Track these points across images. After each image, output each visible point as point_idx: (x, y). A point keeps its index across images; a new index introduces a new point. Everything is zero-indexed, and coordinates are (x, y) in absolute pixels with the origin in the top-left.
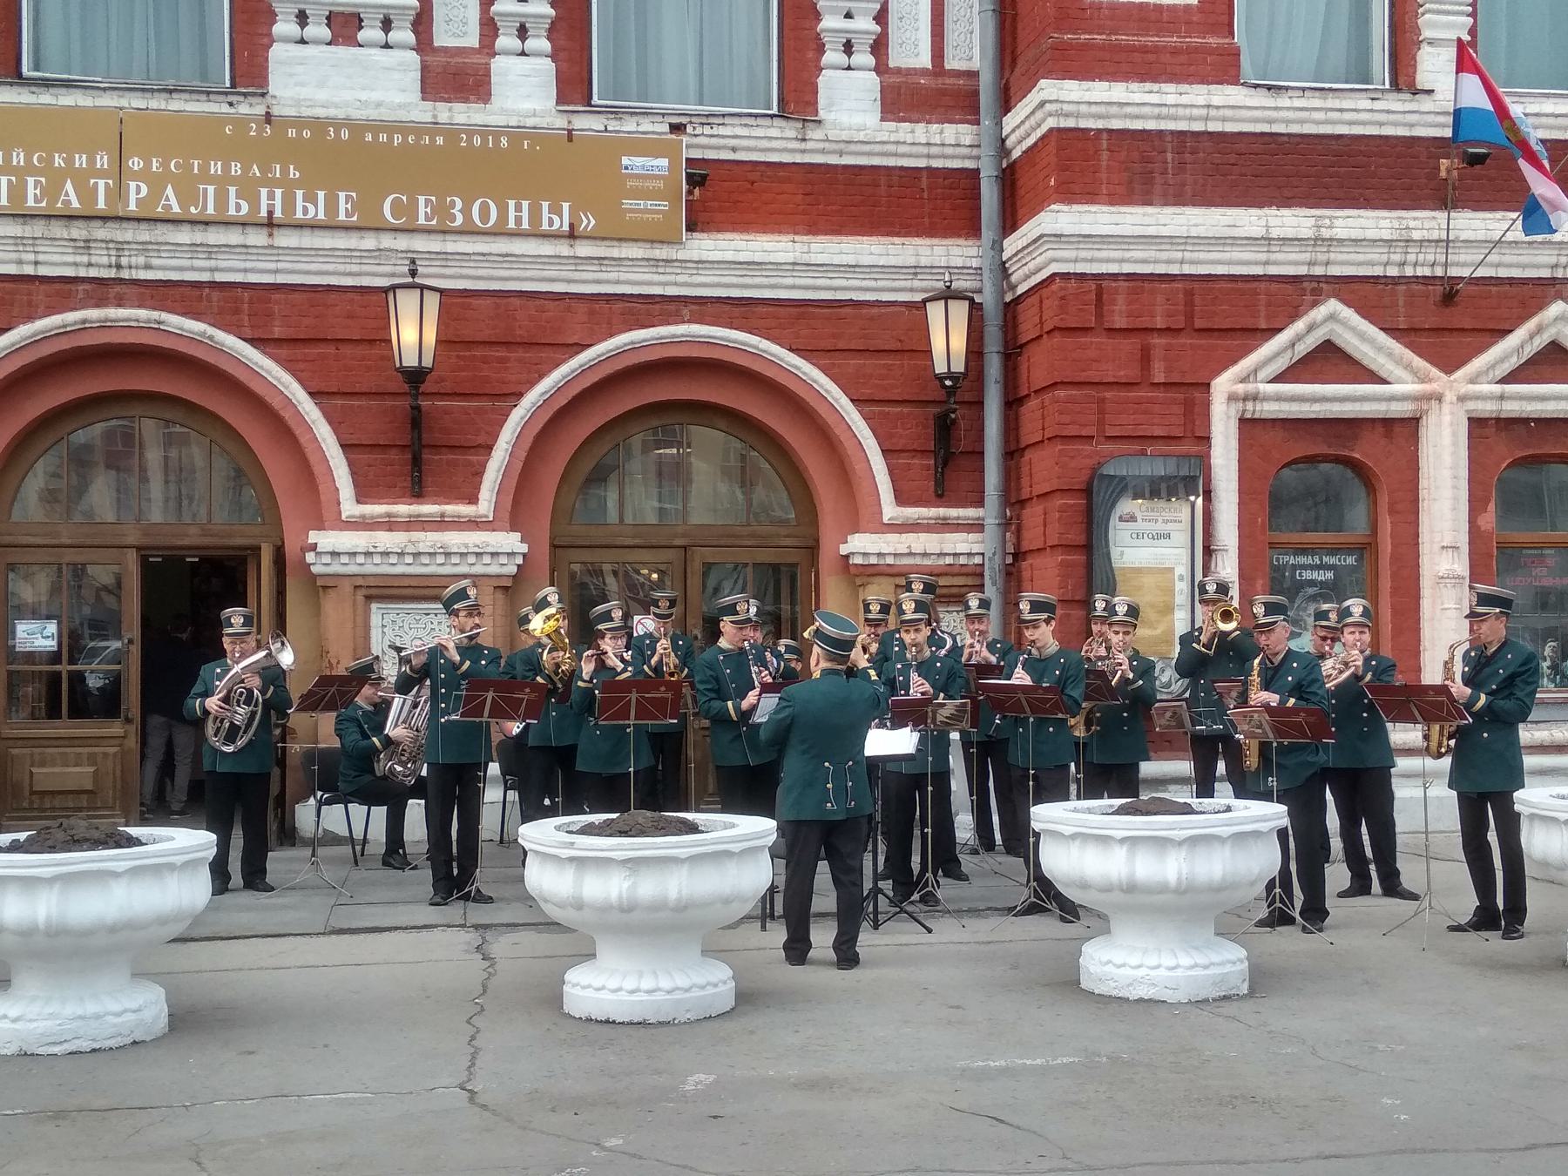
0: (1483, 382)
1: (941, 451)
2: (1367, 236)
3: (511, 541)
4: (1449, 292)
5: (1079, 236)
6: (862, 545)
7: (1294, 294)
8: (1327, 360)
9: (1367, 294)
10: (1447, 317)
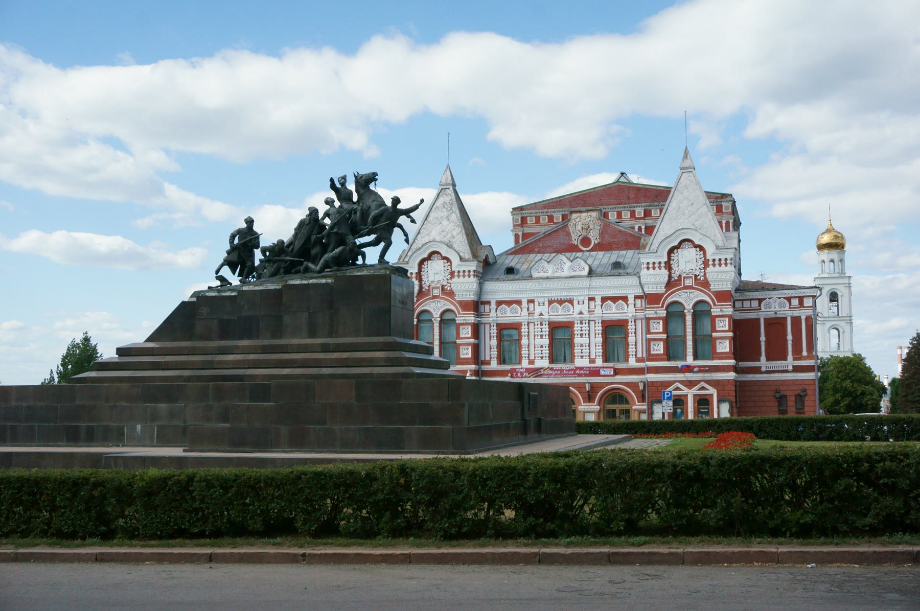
0: (695, 391)
1: (642, 398)
2: (680, 376)
3: (598, 407)
4: (690, 382)
5: (652, 377)
6: (634, 407)
7: (673, 382)
8: (677, 389)
9: (681, 382)
10: (690, 384)
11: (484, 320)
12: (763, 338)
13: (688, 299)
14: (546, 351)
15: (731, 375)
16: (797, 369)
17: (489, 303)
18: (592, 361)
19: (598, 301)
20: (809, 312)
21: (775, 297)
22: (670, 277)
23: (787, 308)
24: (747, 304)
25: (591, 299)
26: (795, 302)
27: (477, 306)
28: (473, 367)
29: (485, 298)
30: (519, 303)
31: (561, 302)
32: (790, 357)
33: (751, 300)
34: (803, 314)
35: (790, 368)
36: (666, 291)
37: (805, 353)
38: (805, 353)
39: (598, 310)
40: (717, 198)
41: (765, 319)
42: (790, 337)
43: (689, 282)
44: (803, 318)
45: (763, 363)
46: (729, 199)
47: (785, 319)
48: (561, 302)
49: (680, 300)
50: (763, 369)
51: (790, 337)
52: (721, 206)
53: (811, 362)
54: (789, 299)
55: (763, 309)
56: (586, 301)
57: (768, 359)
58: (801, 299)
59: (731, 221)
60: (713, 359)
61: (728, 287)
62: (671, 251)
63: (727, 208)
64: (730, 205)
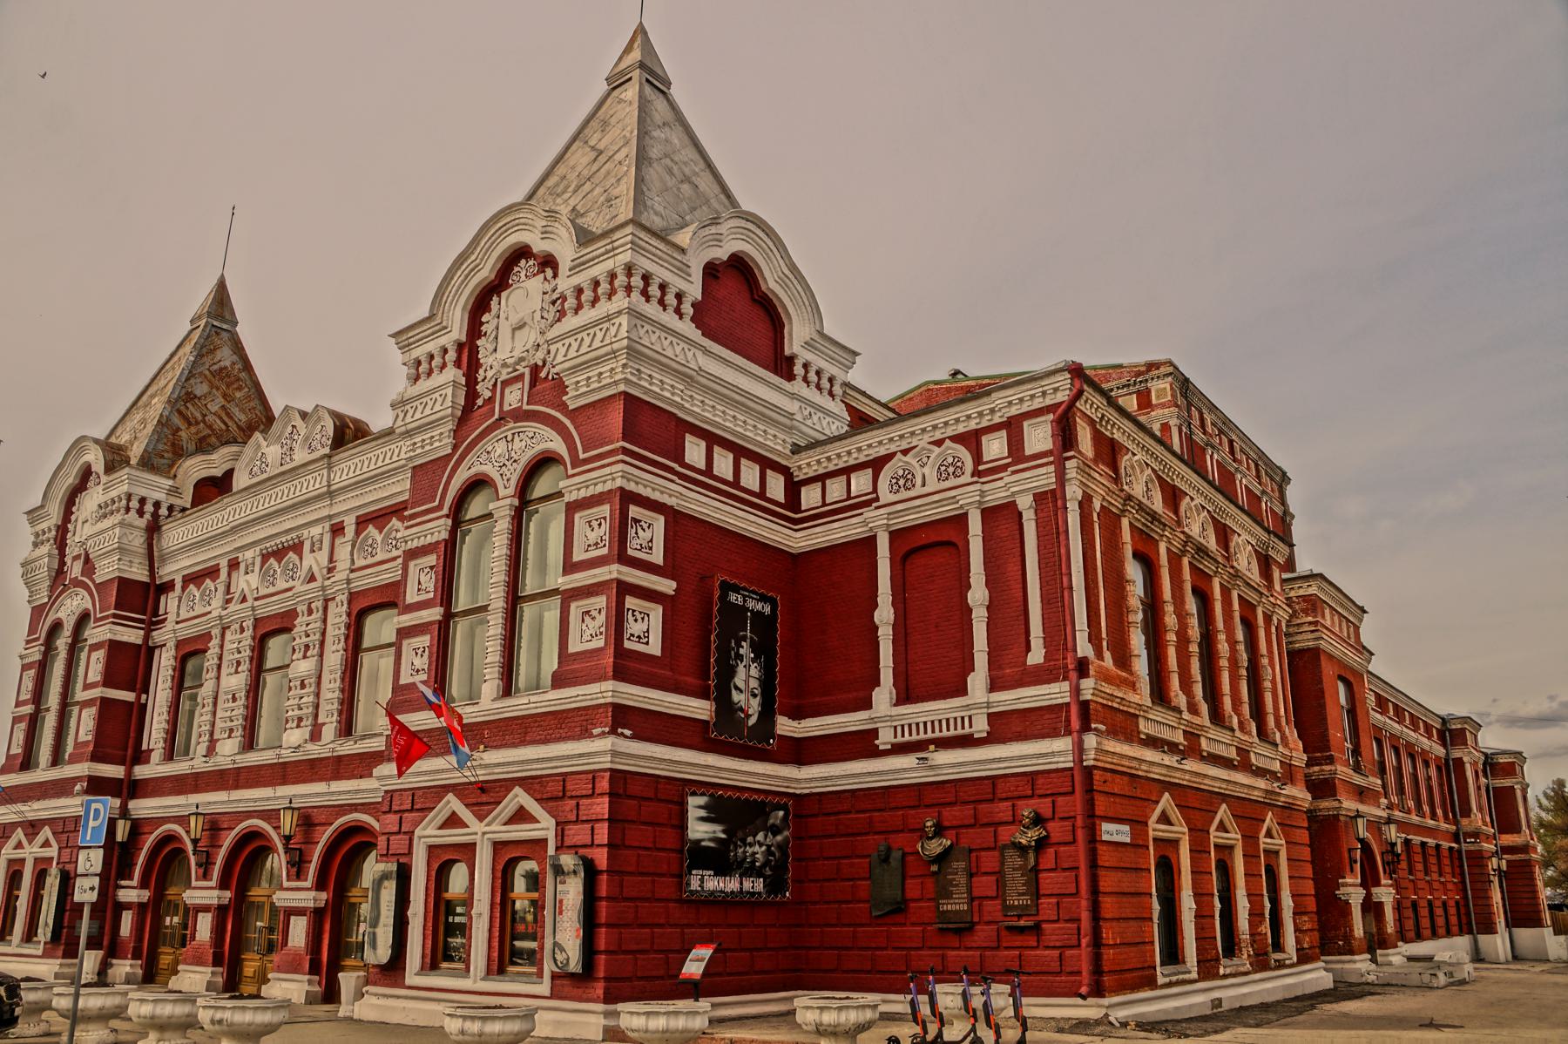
4: (483, 787)
8: (453, 821)
11: (158, 636)
12: (884, 614)
13: (501, 456)
14: (239, 710)
15: (599, 751)
16: (1005, 727)
17: (168, 587)
18: (315, 735)
19: (350, 530)
20: (1044, 478)
21: (922, 442)
22: (472, 394)
23: (967, 478)
24: (836, 489)
25: (338, 530)
26: (995, 447)
27: (140, 598)
28: (83, 769)
29: (168, 571)
30: (213, 572)
31: (279, 554)
32: (978, 680)
33: (847, 471)
34: (1021, 488)
35: (981, 727)
36: (455, 447)
37: (1036, 656)
38: (1036, 656)
39: (343, 562)
40: (1139, 374)
41: (895, 536)
42: (978, 595)
43: (514, 397)
44: (1025, 503)
45: (884, 710)
46: (1163, 370)
47: (961, 520)
48: (279, 554)
49: (490, 470)
50: (885, 739)
51: (978, 595)
52: (1148, 391)
53: (1056, 692)
54: (972, 440)
55: (885, 495)
56: (327, 539)
57: (906, 694)
58: (1013, 427)
59: (1173, 422)
60: (559, 681)
61: (610, 378)
62: (481, 304)
63: (1161, 393)
64: (1165, 384)
